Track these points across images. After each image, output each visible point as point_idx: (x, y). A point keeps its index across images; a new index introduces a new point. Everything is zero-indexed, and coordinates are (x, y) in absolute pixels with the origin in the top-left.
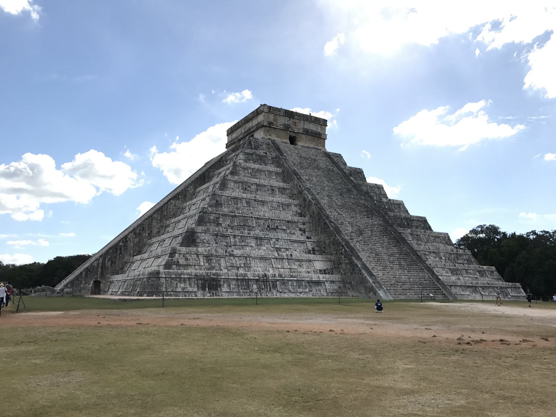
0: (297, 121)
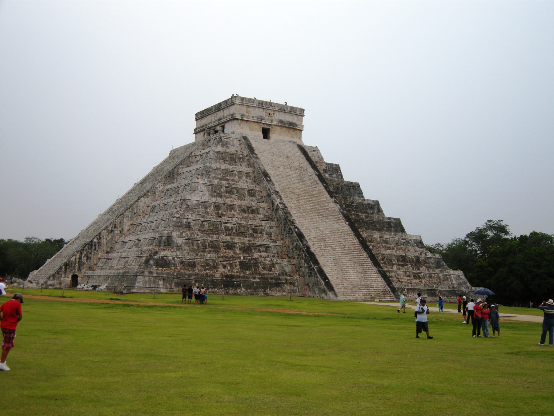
0: (272, 112)
